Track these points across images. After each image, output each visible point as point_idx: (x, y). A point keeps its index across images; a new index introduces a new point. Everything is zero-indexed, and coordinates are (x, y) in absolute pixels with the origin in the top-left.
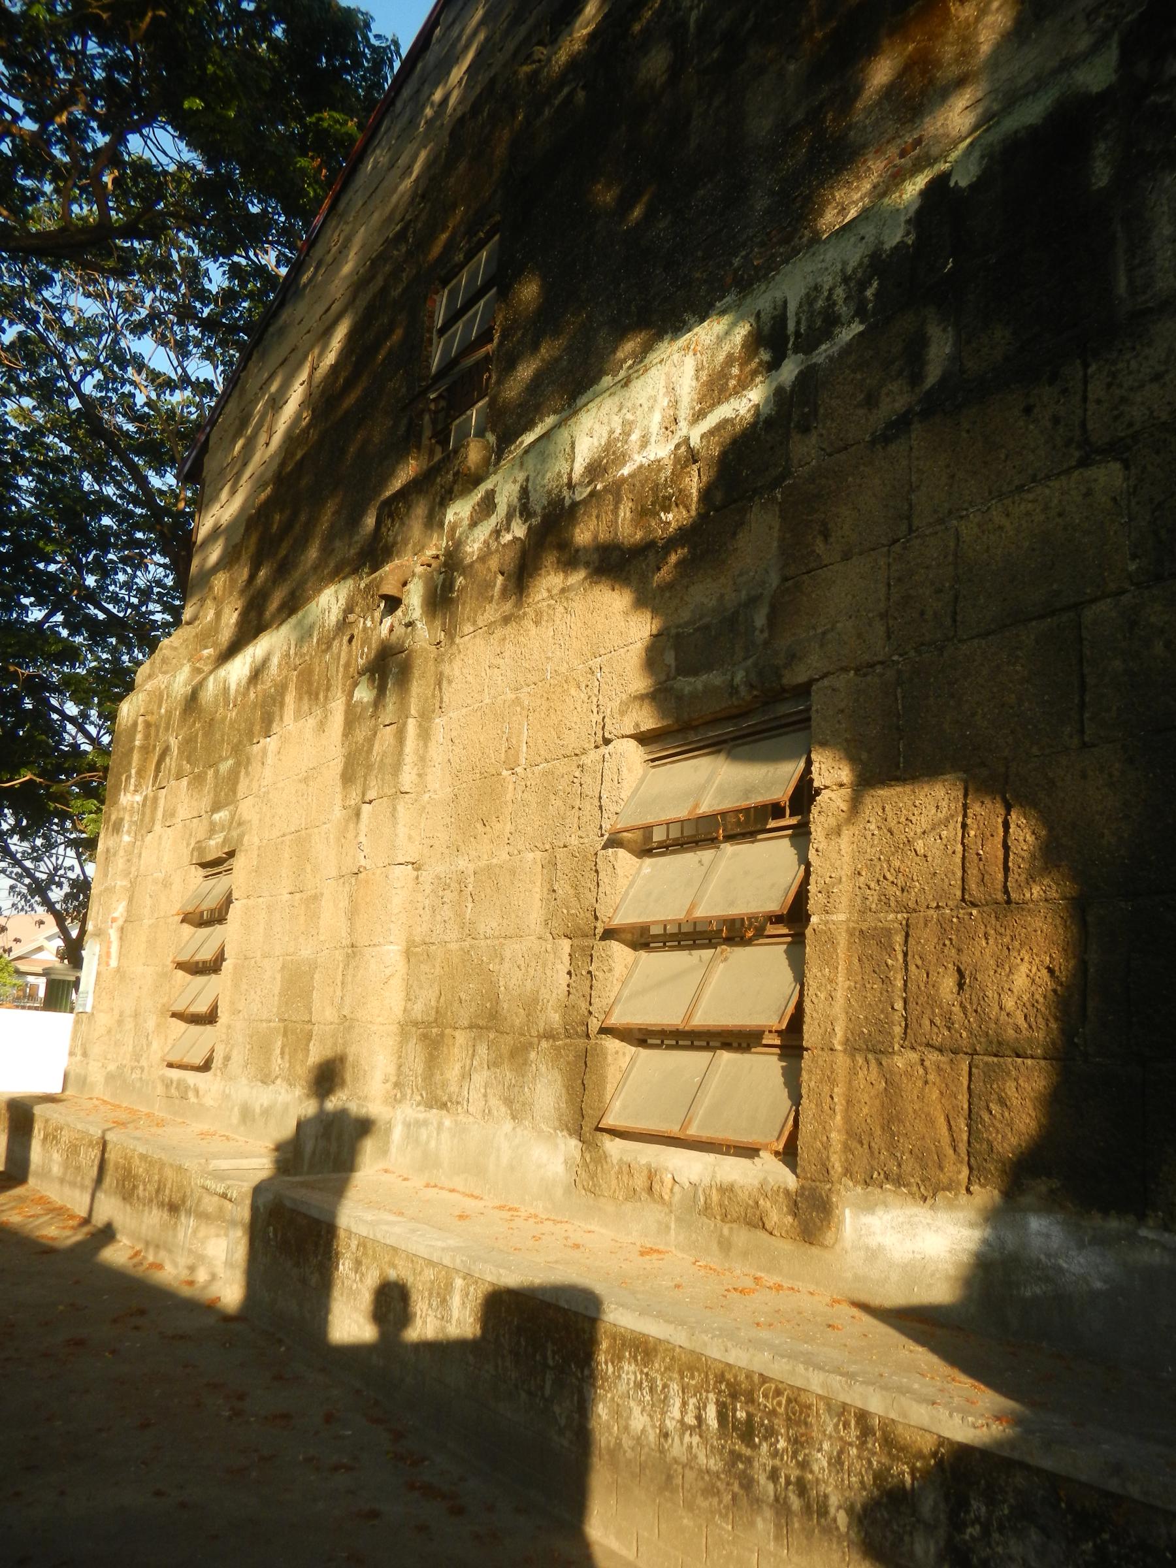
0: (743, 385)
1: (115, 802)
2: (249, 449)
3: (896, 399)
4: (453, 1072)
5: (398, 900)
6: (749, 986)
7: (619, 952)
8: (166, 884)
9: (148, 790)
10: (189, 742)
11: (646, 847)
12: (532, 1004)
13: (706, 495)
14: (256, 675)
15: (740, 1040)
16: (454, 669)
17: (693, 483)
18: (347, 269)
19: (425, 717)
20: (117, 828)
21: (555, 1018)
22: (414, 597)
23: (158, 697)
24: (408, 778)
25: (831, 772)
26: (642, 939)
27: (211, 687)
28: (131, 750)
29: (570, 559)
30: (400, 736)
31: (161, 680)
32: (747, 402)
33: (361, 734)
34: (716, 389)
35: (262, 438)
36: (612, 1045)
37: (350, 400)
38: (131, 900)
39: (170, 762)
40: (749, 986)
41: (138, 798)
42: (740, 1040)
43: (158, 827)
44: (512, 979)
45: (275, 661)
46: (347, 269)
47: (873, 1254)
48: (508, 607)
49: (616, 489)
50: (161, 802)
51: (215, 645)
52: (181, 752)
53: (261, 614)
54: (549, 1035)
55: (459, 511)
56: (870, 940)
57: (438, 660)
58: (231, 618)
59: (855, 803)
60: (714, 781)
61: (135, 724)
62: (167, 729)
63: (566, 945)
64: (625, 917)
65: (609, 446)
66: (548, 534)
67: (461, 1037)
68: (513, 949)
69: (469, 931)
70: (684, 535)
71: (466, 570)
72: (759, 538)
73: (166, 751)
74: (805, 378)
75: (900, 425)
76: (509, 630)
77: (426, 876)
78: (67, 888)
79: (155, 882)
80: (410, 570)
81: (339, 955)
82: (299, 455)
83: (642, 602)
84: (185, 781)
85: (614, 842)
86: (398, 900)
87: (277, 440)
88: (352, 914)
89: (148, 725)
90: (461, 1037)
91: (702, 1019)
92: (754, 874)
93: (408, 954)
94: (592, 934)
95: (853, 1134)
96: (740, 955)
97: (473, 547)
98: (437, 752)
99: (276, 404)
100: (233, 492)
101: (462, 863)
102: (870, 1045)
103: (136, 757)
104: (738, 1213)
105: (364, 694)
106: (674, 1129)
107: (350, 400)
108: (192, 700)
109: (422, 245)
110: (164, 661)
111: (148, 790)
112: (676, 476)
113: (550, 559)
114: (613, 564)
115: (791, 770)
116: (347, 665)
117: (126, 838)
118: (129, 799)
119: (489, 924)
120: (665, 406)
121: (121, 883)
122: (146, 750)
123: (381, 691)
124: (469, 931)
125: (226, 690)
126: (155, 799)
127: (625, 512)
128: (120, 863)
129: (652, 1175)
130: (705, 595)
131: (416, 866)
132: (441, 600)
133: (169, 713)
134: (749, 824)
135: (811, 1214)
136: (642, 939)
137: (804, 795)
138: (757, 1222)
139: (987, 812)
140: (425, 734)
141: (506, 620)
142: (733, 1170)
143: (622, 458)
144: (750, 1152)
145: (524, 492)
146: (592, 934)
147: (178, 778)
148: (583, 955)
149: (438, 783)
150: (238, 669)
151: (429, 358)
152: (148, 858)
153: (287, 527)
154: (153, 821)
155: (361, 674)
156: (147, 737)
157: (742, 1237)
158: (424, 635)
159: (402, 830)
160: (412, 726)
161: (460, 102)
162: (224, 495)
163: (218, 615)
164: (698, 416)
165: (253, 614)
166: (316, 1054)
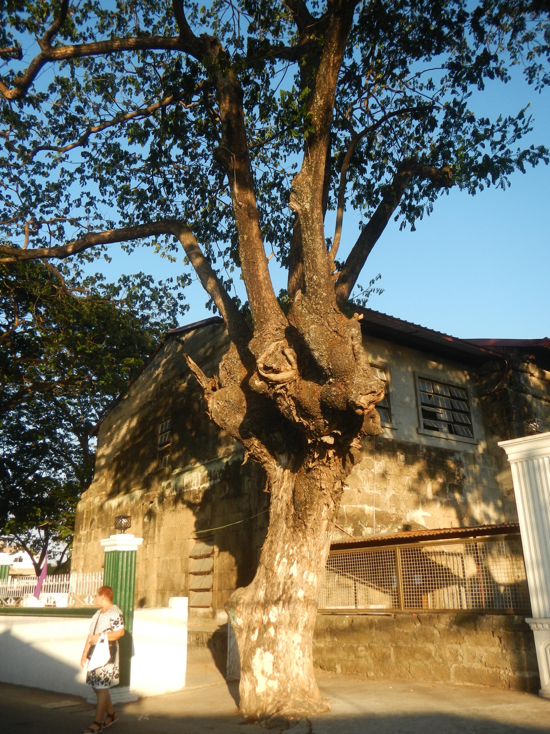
0: (207, 482)
1: (78, 533)
2: (112, 436)
3: (223, 494)
4: (166, 600)
5: (155, 565)
6: (206, 581)
7: (192, 576)
8: (96, 557)
9: (88, 530)
10: (100, 519)
11: (196, 558)
12: (179, 585)
13: (202, 498)
14: (119, 505)
15: (207, 590)
16: (165, 518)
17: (201, 495)
18: (137, 401)
19: (159, 527)
20: (80, 540)
21: (183, 588)
22: (156, 501)
23: (90, 504)
24: (156, 539)
25: (216, 549)
26: (195, 574)
27: (106, 506)
28: (83, 519)
29: (184, 502)
30: (154, 530)
31: (91, 499)
32: (207, 485)
33: (146, 529)
34: (203, 481)
35: (116, 436)
36: (191, 592)
37: (139, 440)
38: (85, 560)
39: (95, 523)
40: (206, 581)
41: (86, 532)
42: (207, 590)
43: (92, 540)
44: (176, 580)
45: (124, 503)
46: (137, 401)
47: (220, 619)
48: (174, 508)
49: (190, 491)
50: (93, 534)
51: (105, 491)
52: (98, 521)
53: (119, 486)
54: (182, 591)
55: (164, 484)
56: (220, 575)
57: (161, 515)
58: (110, 485)
59: (219, 554)
60: (203, 548)
61: (83, 511)
62: (93, 513)
63: (184, 575)
64: (192, 571)
65: (189, 483)
66: (180, 496)
67: (168, 592)
68: (176, 575)
69: (169, 571)
70: (200, 504)
71: (166, 498)
72: (208, 508)
73: (93, 520)
74: (214, 484)
75: (223, 498)
76: (174, 513)
77: (160, 560)
78: (31, 543)
79: (93, 556)
80: (155, 492)
81: (144, 577)
82: (127, 447)
83: (195, 514)
84: (100, 530)
85: (190, 557)
86: (155, 565)
87: (120, 438)
88: (146, 568)
89: (87, 512)
90: (168, 592)
91: (202, 587)
92: (206, 564)
93: (158, 576)
94: (188, 573)
95: (218, 602)
96: (208, 576)
97: (167, 492)
98: (162, 539)
99: (119, 428)
100: (108, 446)
101: (167, 558)
102: (220, 590)
103: (84, 521)
104: (206, 616)
105: (146, 519)
106: (198, 605)
107: (139, 440)
108: (101, 507)
109: (155, 411)
110: (91, 493)
111: (88, 530)
112: (199, 493)
113: (180, 501)
114: (190, 505)
115: (212, 547)
116: (142, 510)
117: (83, 544)
118: (83, 533)
119: (172, 571)
120: (196, 479)
121: (82, 556)
122: (87, 519)
123: (150, 519)
124: (169, 571)
125: (111, 507)
126: (91, 533)
127: (192, 497)
128: (81, 550)
129: (196, 612)
130: (202, 516)
131: (159, 558)
132: (161, 501)
133: (94, 509)
134: (208, 556)
135: (214, 614)
136: (195, 574)
137: (213, 552)
138: (208, 617)
139: (231, 557)
140: (159, 531)
141: (174, 511)
142: (206, 610)
143: (191, 487)
144: (207, 607)
145: (176, 486)
146: (188, 573)
147: (98, 528)
148: (186, 576)
149: (162, 542)
150: (114, 503)
151: (157, 440)
152: (89, 549)
153: (125, 466)
154: (91, 539)
155: (146, 515)
156: (87, 515)
157: (207, 620)
158: (158, 508)
159: (155, 551)
160: (156, 529)
161: (163, 378)
162: (105, 446)
163: (106, 483)
164: (201, 484)
165: (116, 486)
166: (139, 598)
